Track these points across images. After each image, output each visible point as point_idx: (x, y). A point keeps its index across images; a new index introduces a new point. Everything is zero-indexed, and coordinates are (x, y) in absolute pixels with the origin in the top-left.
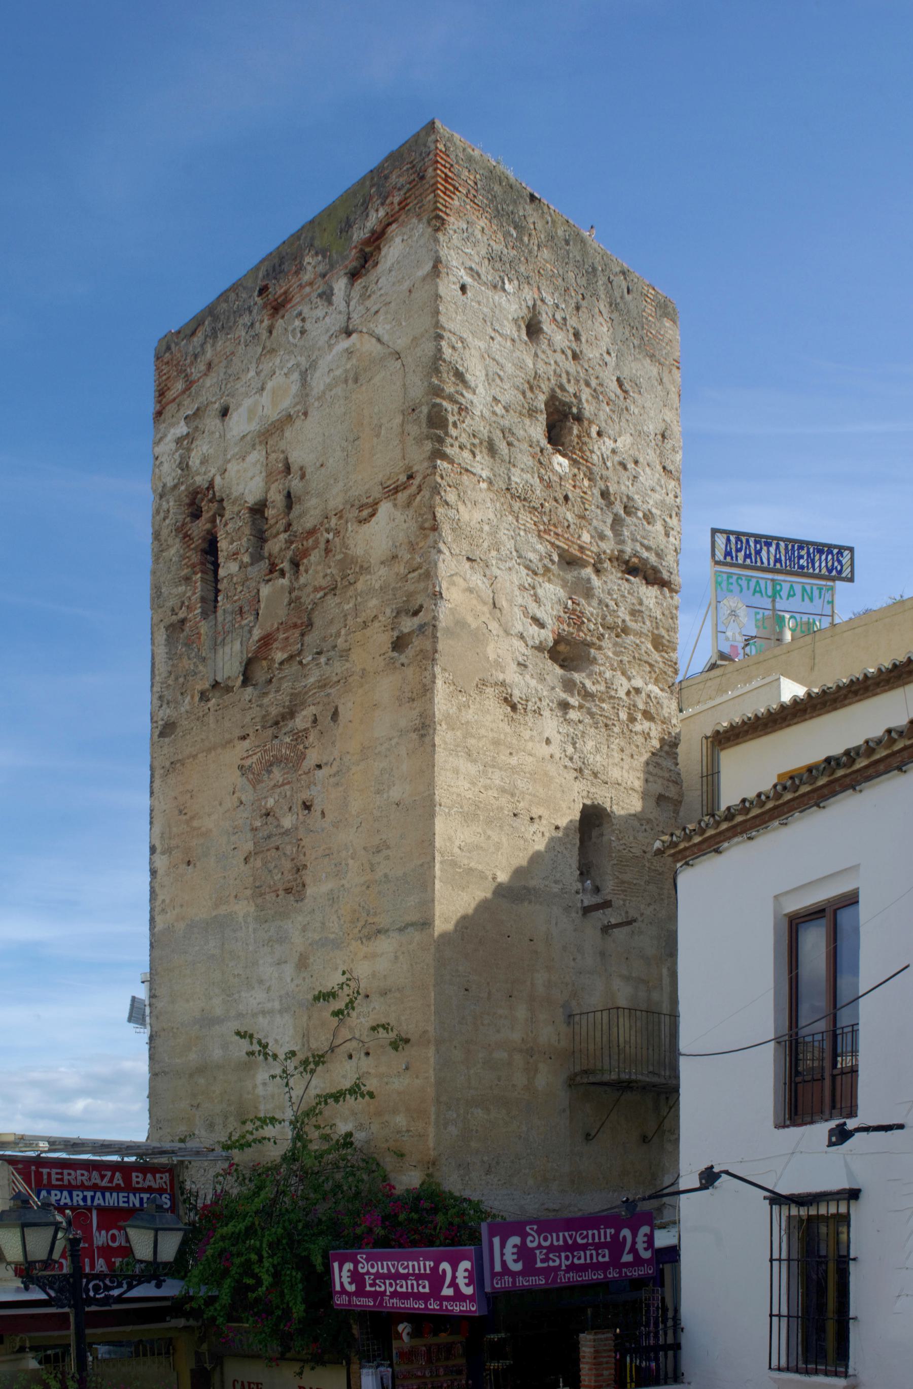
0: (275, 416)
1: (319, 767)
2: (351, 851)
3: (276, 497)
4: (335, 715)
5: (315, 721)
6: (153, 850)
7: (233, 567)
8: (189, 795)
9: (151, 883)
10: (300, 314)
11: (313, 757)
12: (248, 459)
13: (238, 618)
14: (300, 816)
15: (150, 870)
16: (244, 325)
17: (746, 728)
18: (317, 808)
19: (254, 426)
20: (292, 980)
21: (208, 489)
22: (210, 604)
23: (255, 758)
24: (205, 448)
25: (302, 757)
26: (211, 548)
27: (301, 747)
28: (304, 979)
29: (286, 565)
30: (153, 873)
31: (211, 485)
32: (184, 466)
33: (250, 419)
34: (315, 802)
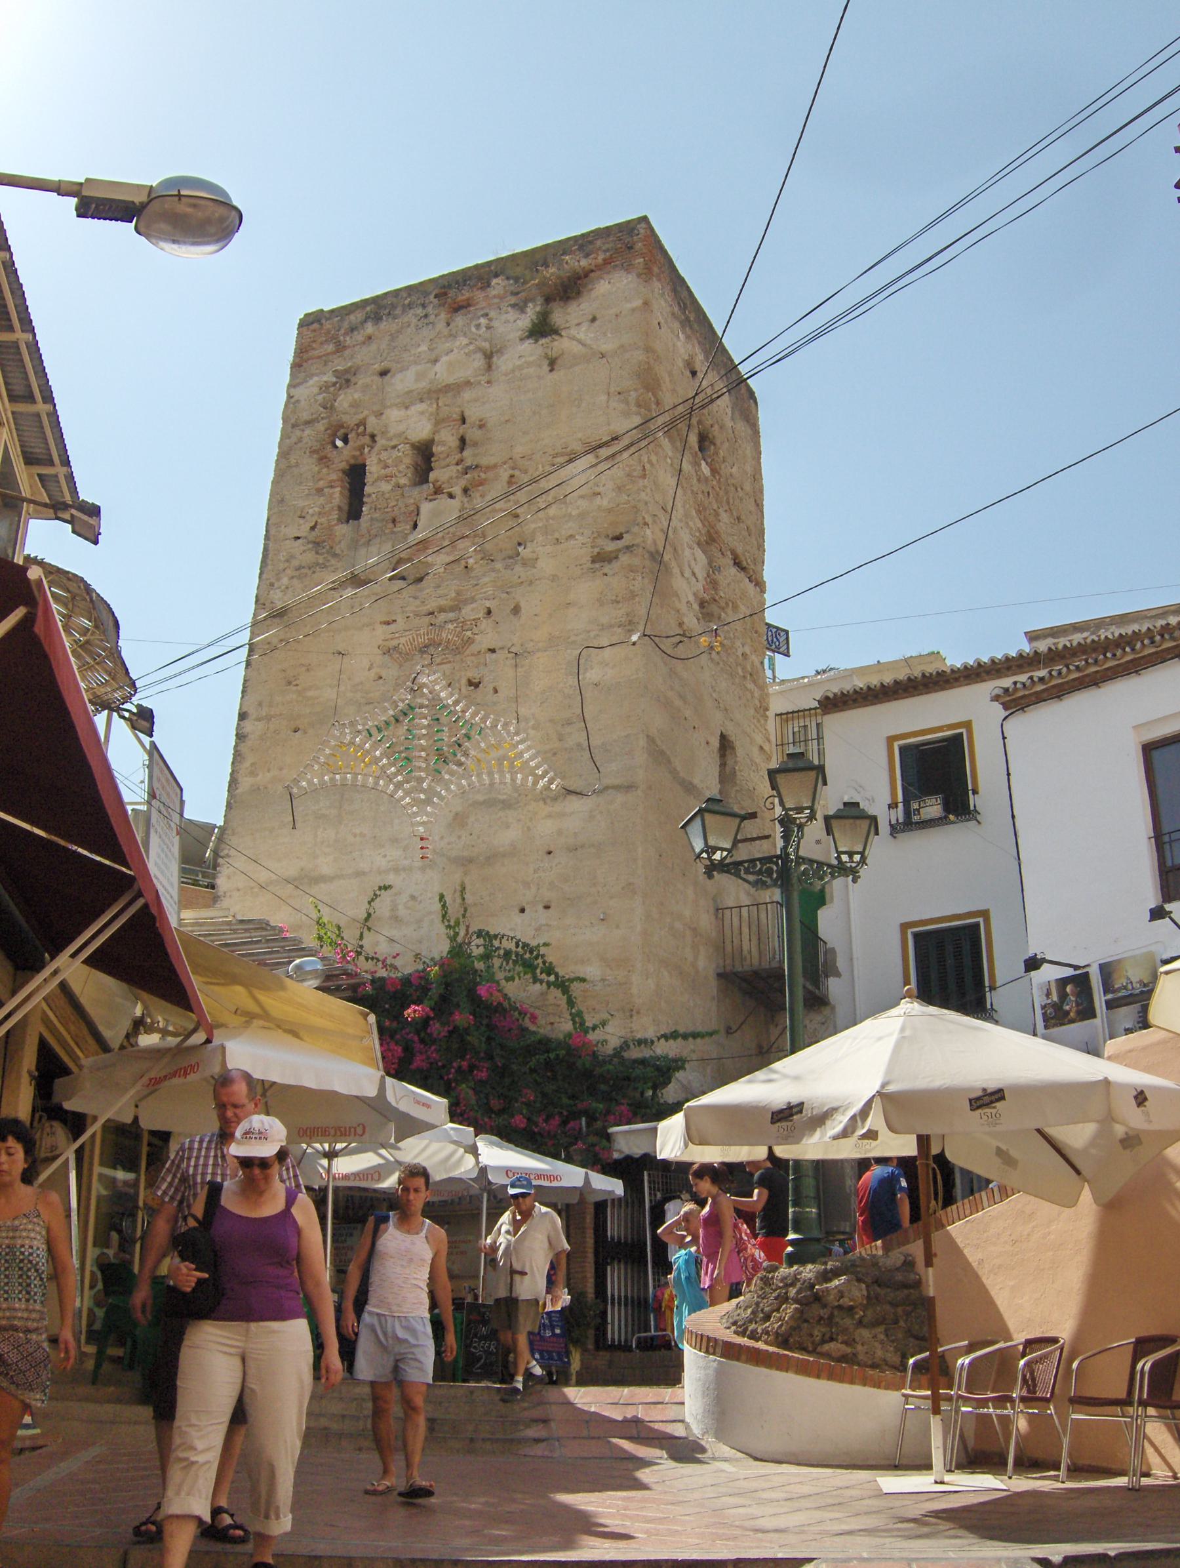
0: (451, 380)
1: (493, 651)
2: (532, 723)
3: (447, 439)
4: (516, 610)
5: (489, 612)
6: (242, 716)
7: (386, 487)
8: (304, 669)
9: (236, 746)
10: (487, 315)
11: (485, 640)
12: (413, 408)
13: (391, 525)
14: (463, 690)
15: (237, 735)
16: (416, 315)
17: (1021, 662)
18: (487, 687)
19: (423, 384)
20: (442, 838)
21: (358, 425)
22: (353, 511)
23: (403, 640)
24: (356, 396)
25: (470, 641)
26: (356, 475)
27: (469, 633)
28: (459, 837)
29: (457, 490)
30: (240, 737)
31: (363, 423)
32: (329, 407)
33: (417, 380)
34: (486, 679)
